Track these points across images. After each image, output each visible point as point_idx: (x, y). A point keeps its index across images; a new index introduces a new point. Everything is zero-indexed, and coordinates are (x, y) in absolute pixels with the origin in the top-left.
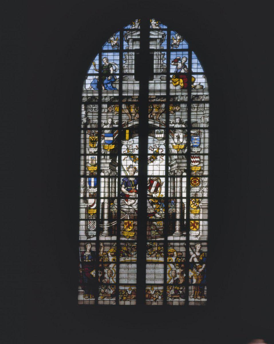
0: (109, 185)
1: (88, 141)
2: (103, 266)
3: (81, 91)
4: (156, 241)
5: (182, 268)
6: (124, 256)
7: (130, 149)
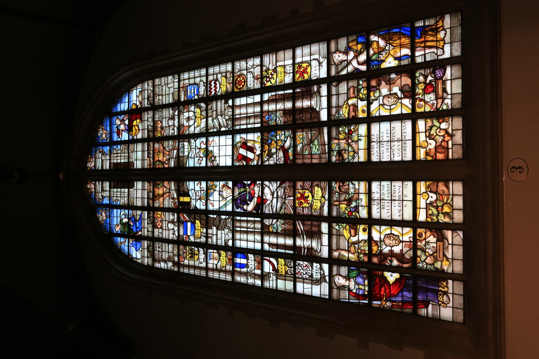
1: (192, 263)
2: (375, 255)
3: (142, 265)
4: (329, 144)
5: (379, 84)
6: (357, 208)
7: (201, 195)
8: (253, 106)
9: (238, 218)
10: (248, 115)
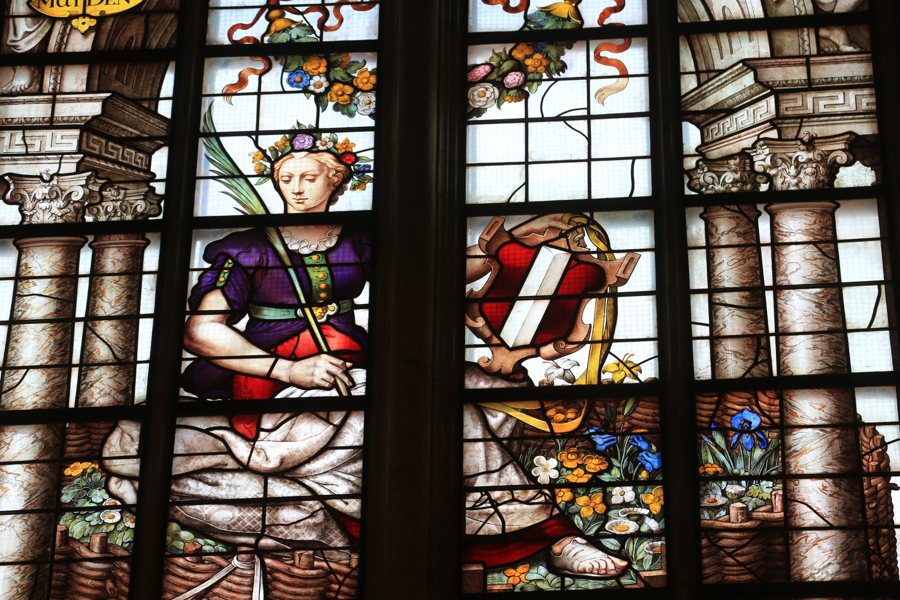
0: (66, 300)
8: (826, 326)
9: (151, 259)
10: (769, 296)
